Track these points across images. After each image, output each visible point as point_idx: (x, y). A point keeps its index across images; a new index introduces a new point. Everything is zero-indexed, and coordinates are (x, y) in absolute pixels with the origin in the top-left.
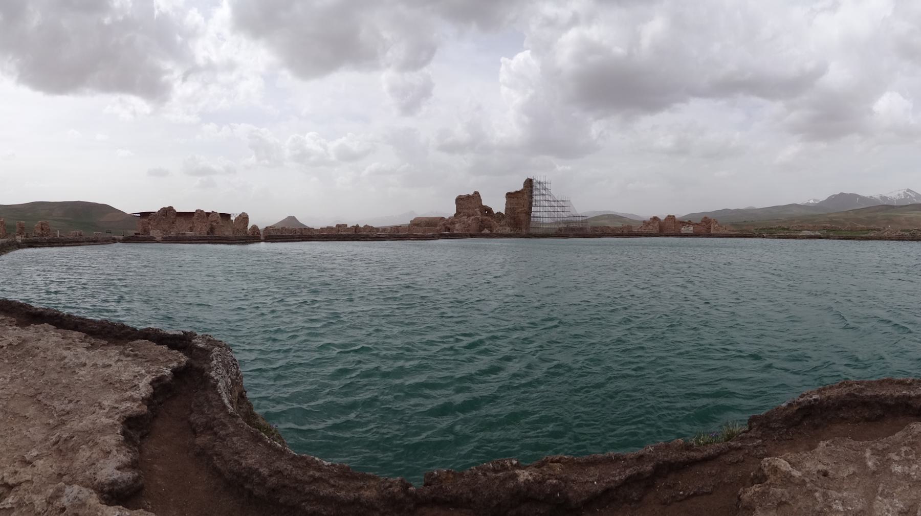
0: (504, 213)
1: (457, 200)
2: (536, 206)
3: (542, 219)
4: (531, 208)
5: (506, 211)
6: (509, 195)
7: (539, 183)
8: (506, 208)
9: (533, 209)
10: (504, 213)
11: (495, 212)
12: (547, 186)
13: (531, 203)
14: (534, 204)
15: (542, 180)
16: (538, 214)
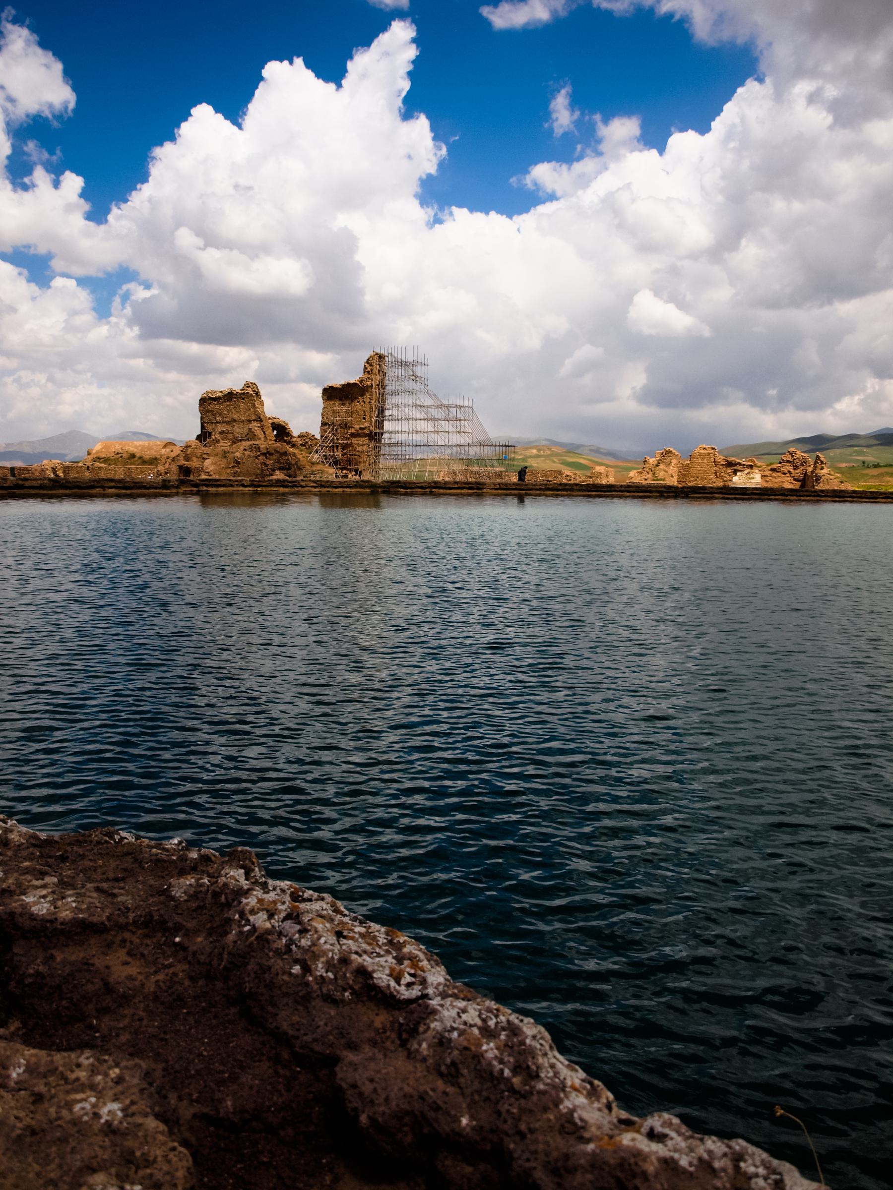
0: (318, 436)
1: (203, 401)
2: (393, 419)
3: (409, 450)
4: (380, 425)
5: (323, 431)
6: (330, 393)
7: (403, 364)
8: (324, 424)
9: (387, 426)
10: (318, 436)
11: (295, 433)
12: (419, 371)
13: (382, 411)
14: (387, 413)
15: (410, 358)
16: (399, 438)
